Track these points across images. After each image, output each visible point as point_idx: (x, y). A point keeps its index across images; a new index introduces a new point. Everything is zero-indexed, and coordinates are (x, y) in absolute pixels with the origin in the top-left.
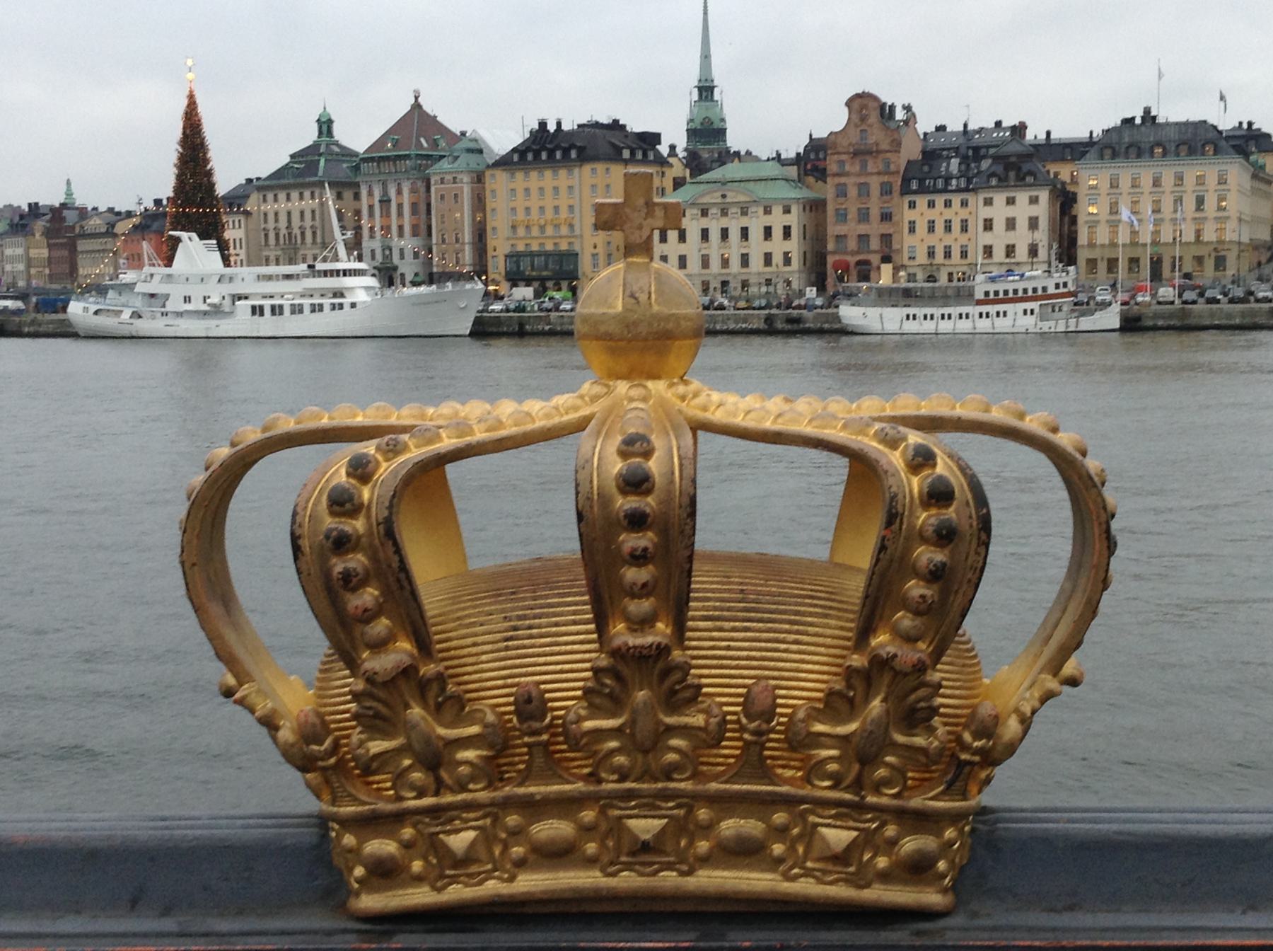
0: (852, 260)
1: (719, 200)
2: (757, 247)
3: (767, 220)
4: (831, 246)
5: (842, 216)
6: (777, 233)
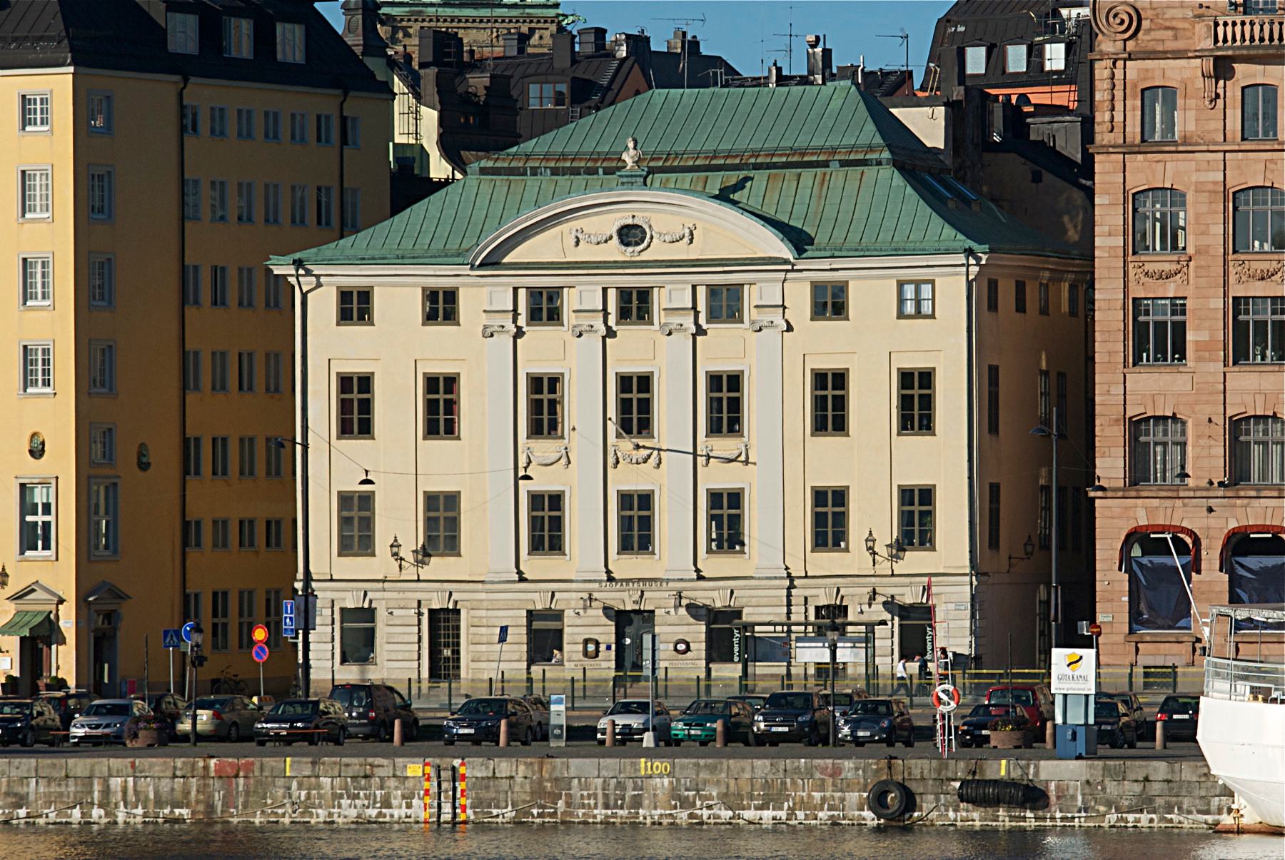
0: (1212, 524)
1: (615, 251)
2: (777, 463)
3: (826, 345)
4: (1110, 464)
5: (1159, 339)
6: (872, 402)
